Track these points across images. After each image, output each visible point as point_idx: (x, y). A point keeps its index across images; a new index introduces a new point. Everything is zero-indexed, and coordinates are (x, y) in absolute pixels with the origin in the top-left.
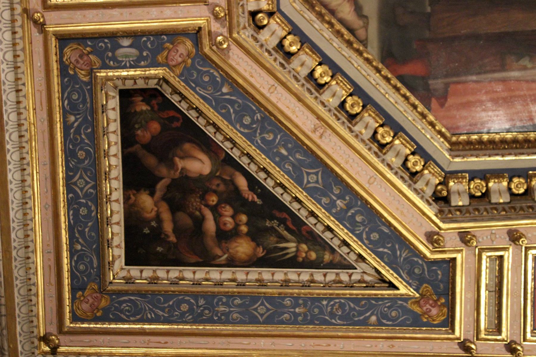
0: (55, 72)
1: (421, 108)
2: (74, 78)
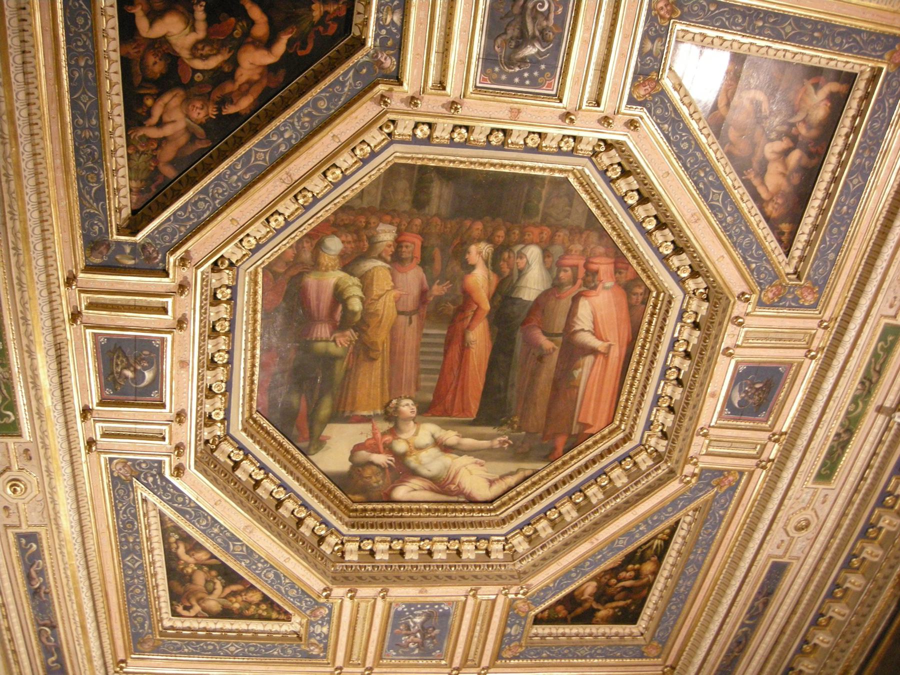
0: (516, 661)
1: (589, 442)
2: (521, 653)
